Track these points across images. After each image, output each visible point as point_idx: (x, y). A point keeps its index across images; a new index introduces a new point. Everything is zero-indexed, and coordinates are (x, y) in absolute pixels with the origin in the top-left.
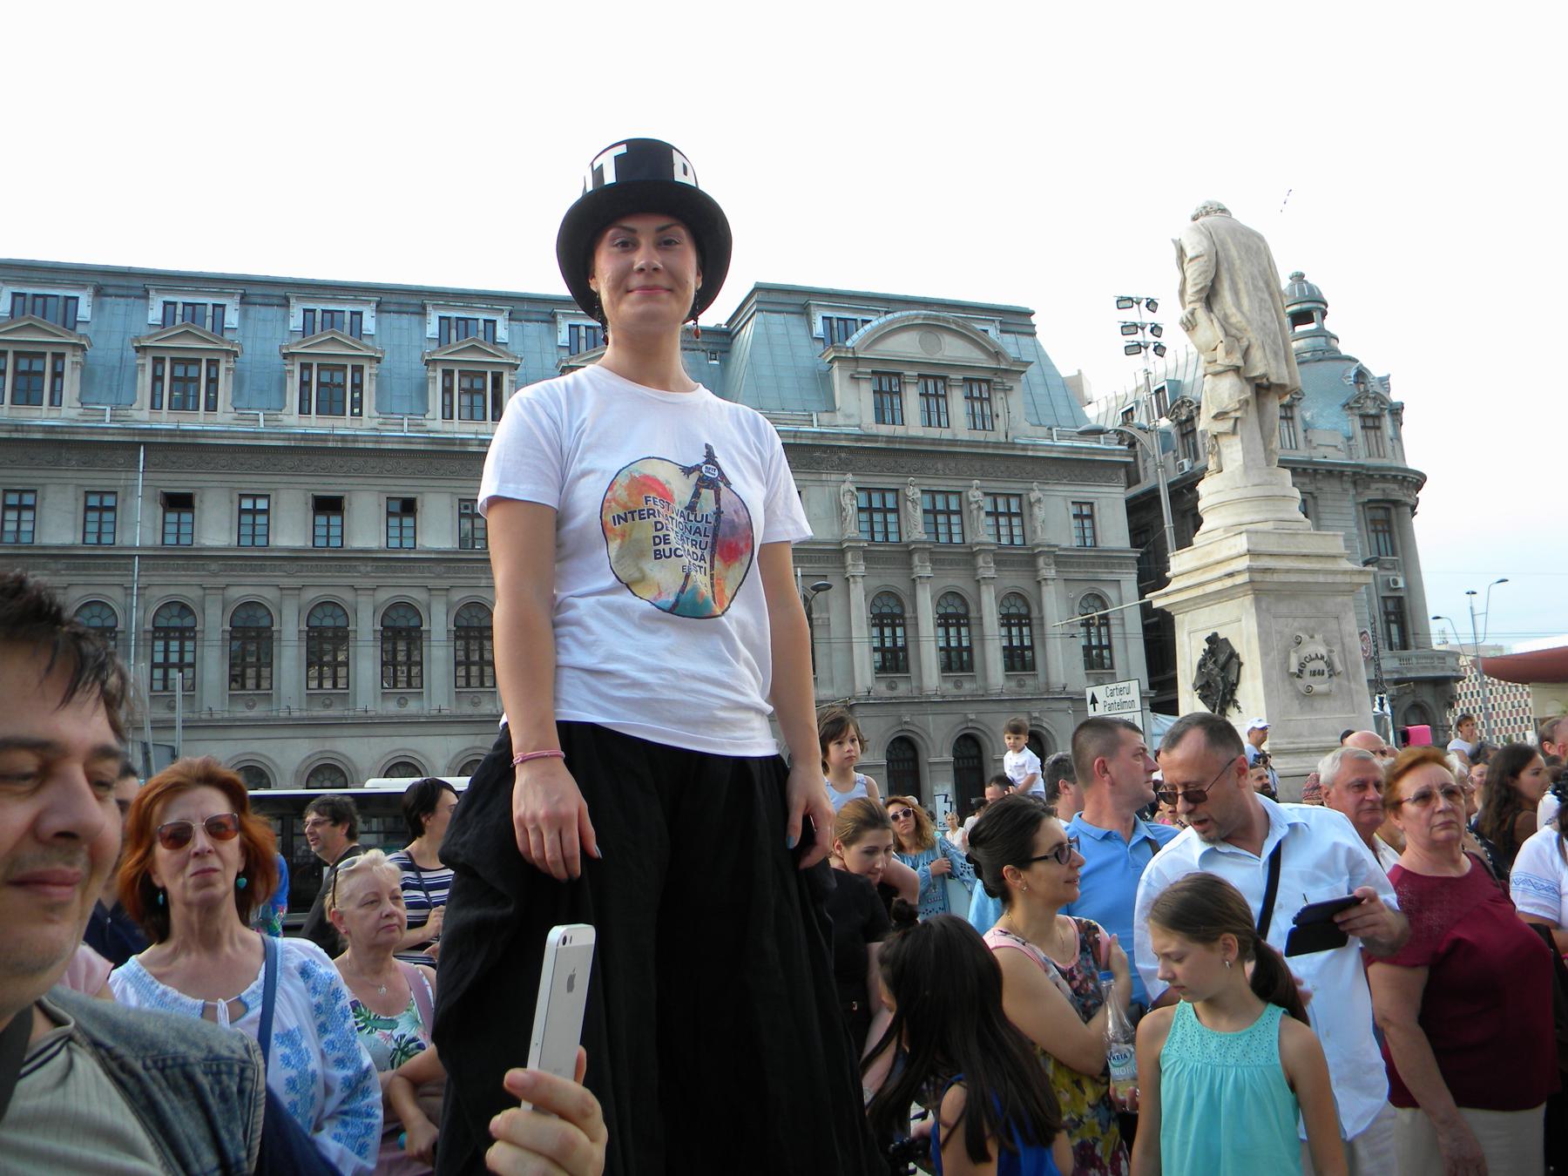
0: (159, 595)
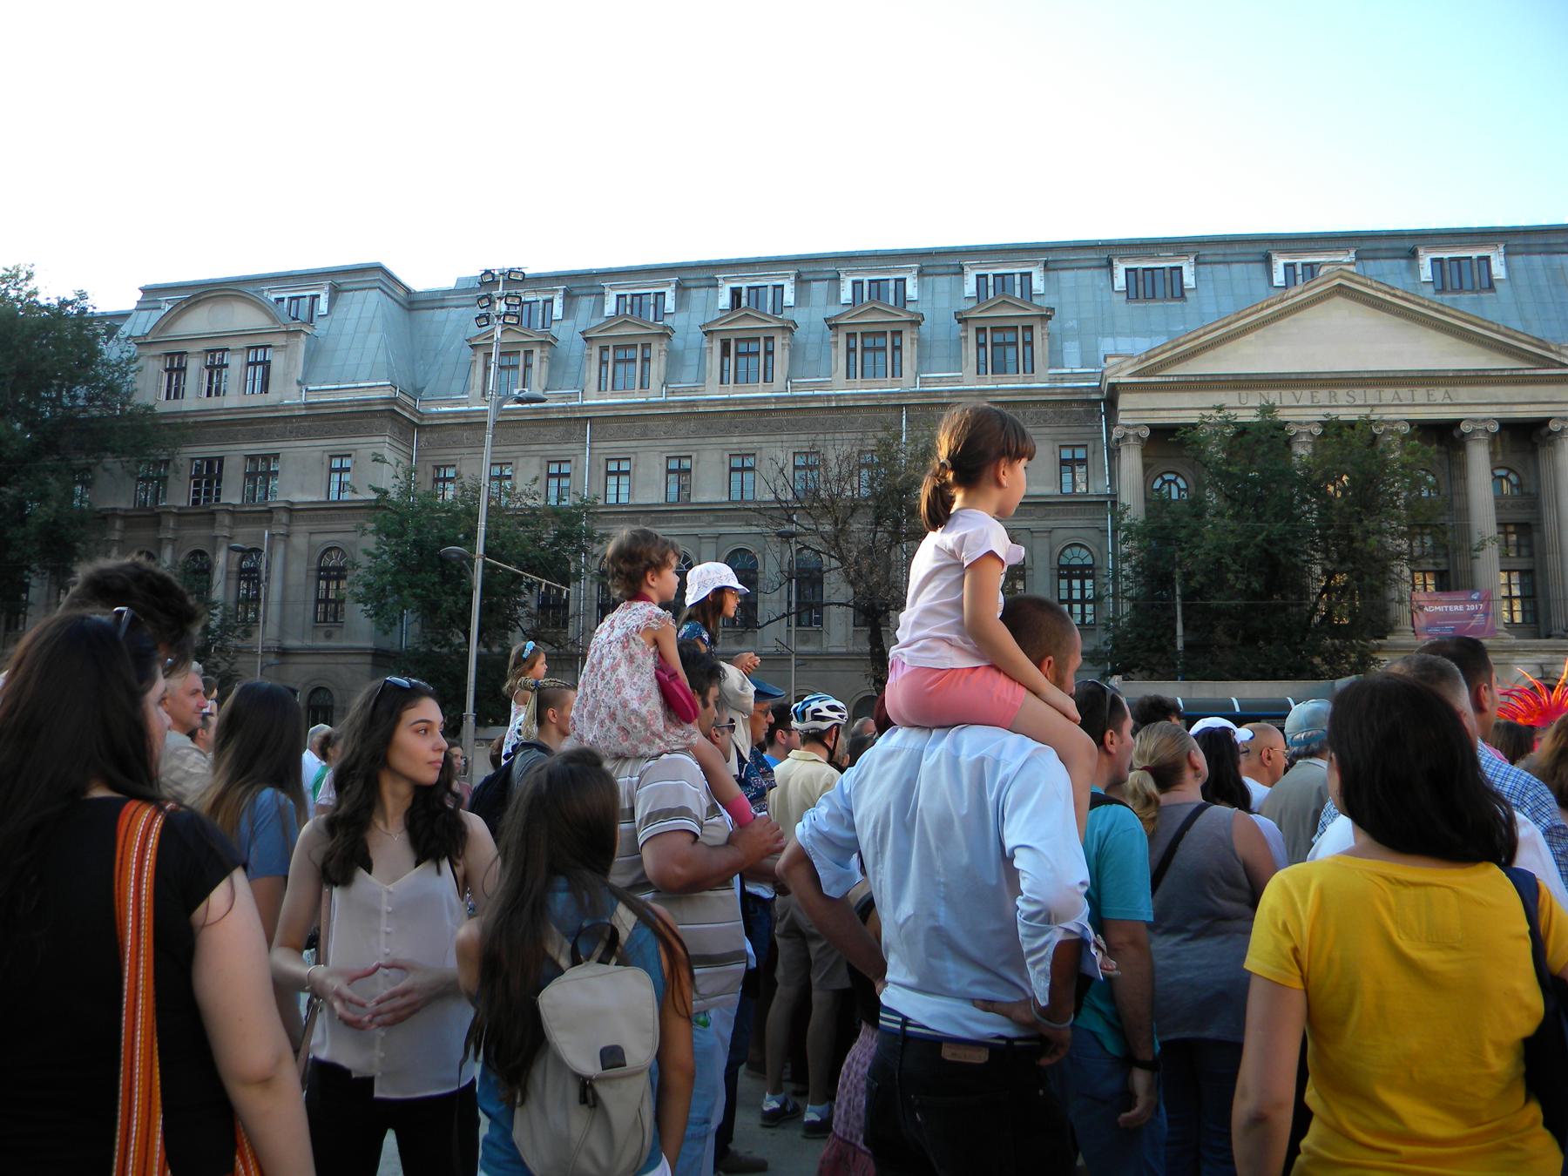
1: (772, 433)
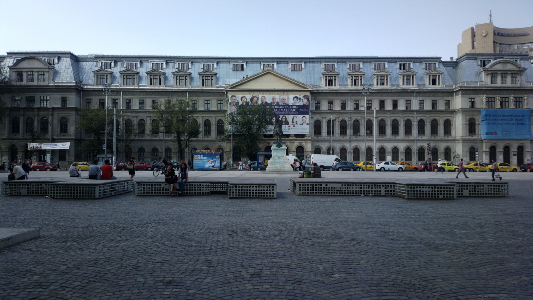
0: (354, 118)
1: (161, 96)
